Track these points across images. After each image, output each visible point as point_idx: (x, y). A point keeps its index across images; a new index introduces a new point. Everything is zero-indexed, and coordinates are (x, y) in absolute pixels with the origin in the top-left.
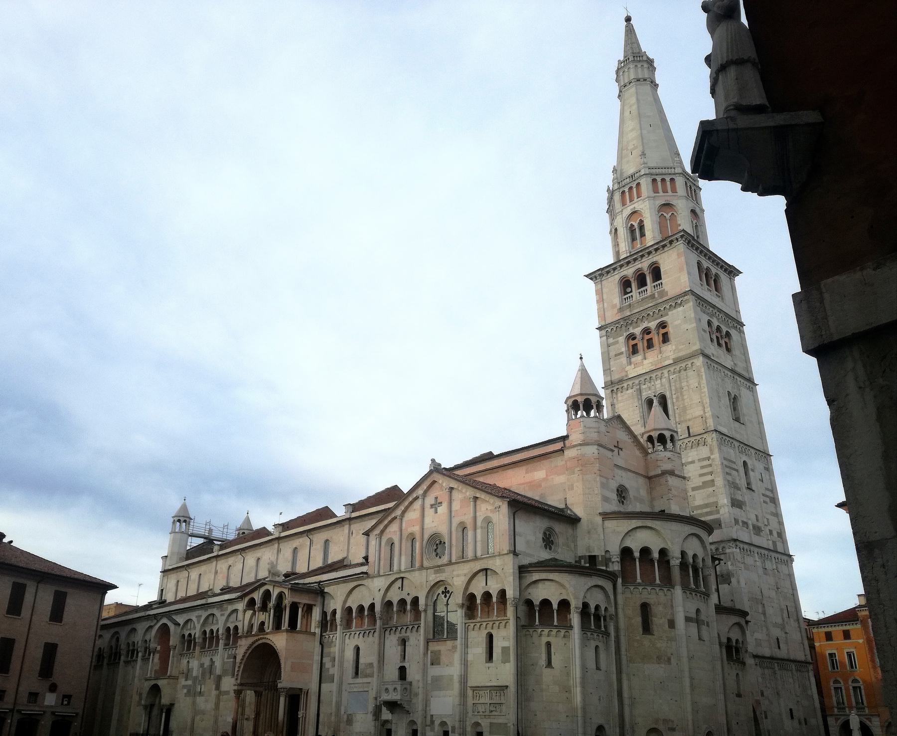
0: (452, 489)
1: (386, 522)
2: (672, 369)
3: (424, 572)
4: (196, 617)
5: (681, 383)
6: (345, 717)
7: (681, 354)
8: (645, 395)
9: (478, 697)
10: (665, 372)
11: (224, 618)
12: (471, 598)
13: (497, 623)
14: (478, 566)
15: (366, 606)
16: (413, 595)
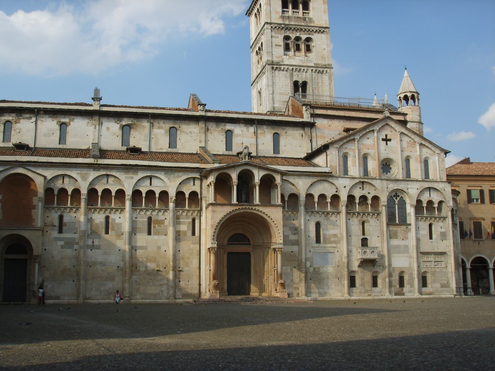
0: (402, 133)
1: (345, 141)
2: (314, 69)
3: (385, 182)
4: (78, 174)
5: (318, 80)
6: (311, 269)
7: (319, 62)
8: (295, 79)
9: (425, 258)
10: (310, 69)
11: (135, 181)
12: (419, 202)
13: (438, 219)
14: (427, 185)
15: (329, 195)
16: (373, 193)
